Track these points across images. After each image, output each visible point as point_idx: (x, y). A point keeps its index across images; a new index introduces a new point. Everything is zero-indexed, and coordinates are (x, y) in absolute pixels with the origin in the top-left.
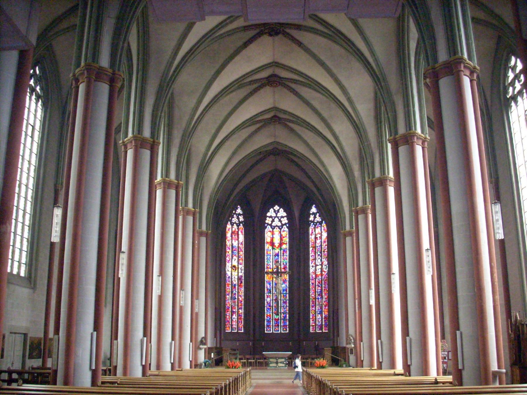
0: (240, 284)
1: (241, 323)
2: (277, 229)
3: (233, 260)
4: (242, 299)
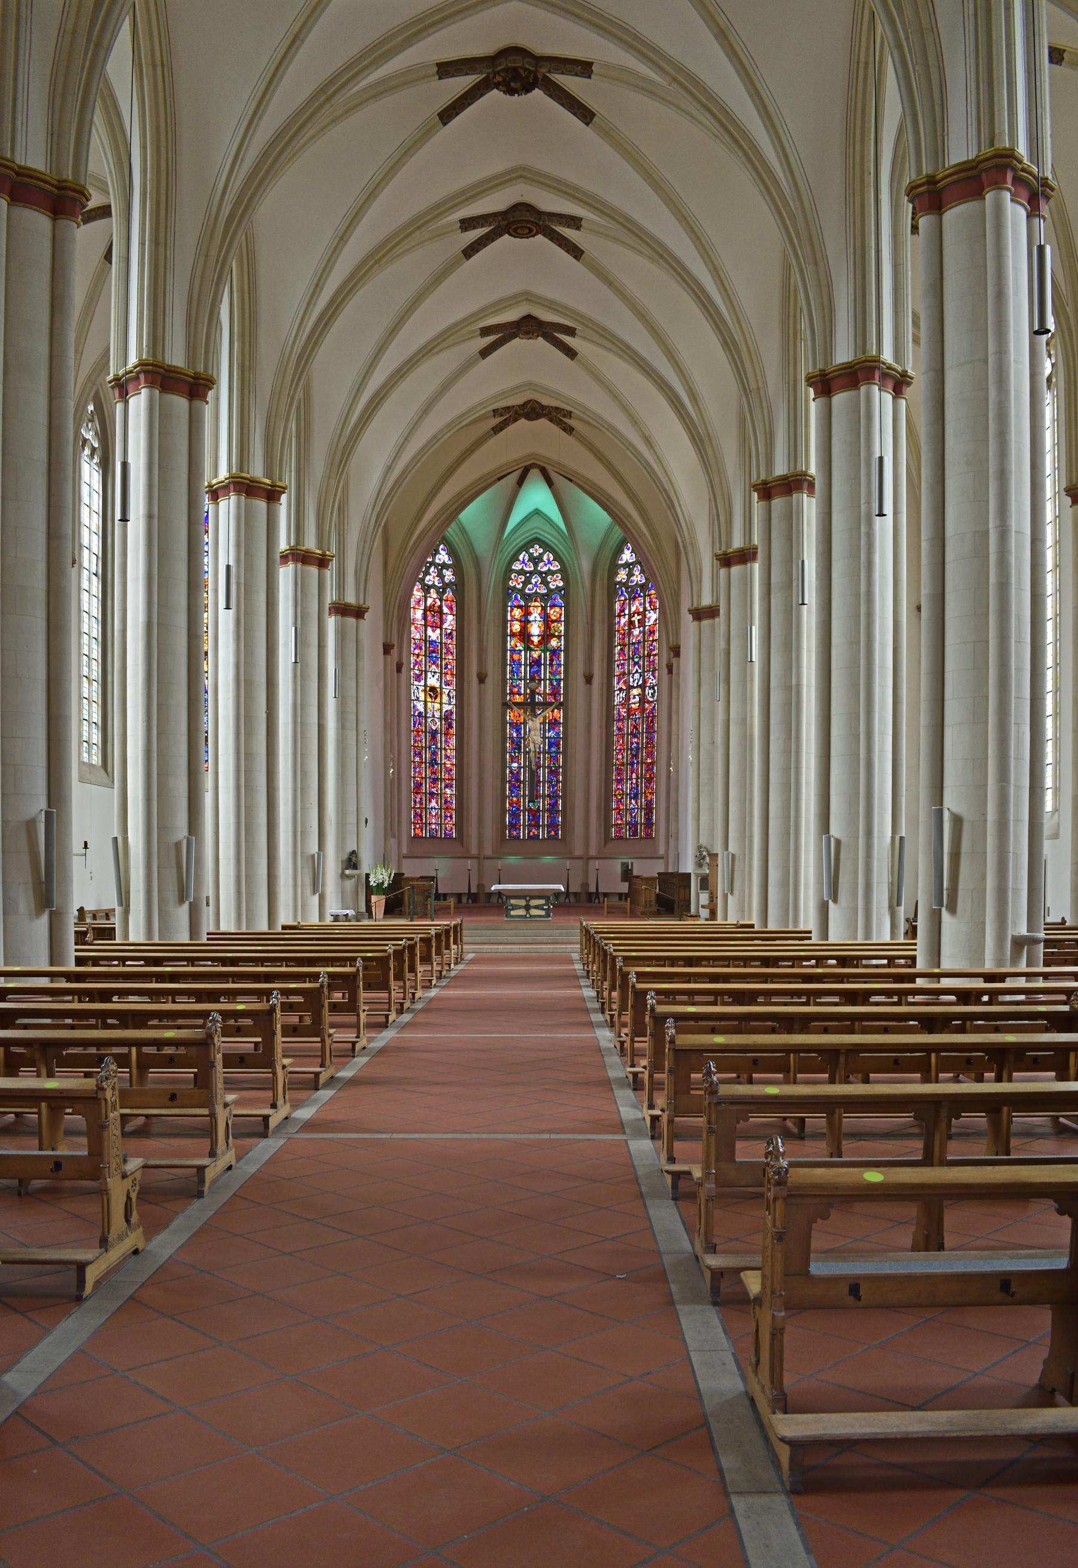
0: (447, 729)
1: (449, 819)
3: (429, 675)
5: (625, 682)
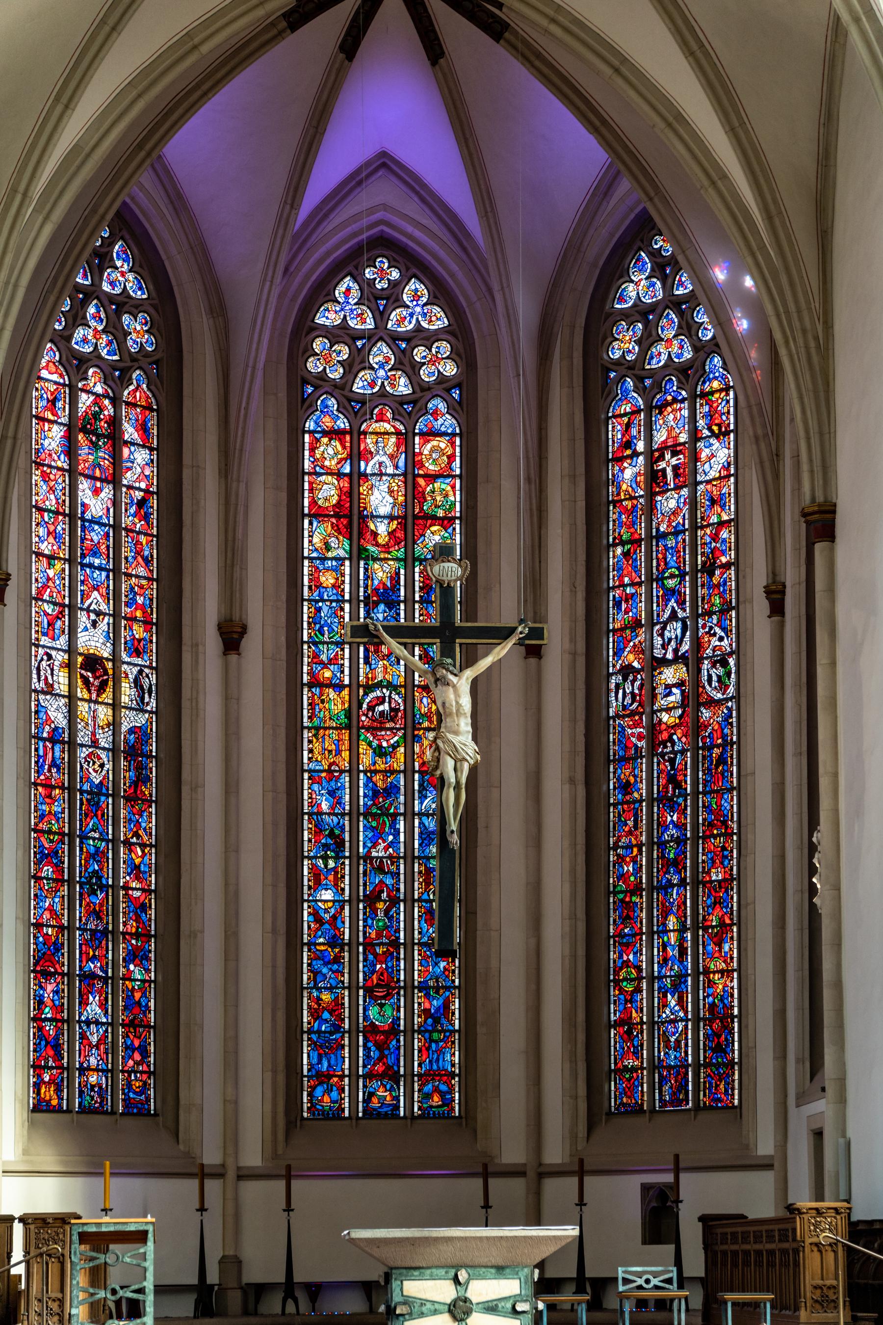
1: (137, 1056)
2: (381, 418)
3: (83, 619)
4: (146, 891)
5: (638, 650)
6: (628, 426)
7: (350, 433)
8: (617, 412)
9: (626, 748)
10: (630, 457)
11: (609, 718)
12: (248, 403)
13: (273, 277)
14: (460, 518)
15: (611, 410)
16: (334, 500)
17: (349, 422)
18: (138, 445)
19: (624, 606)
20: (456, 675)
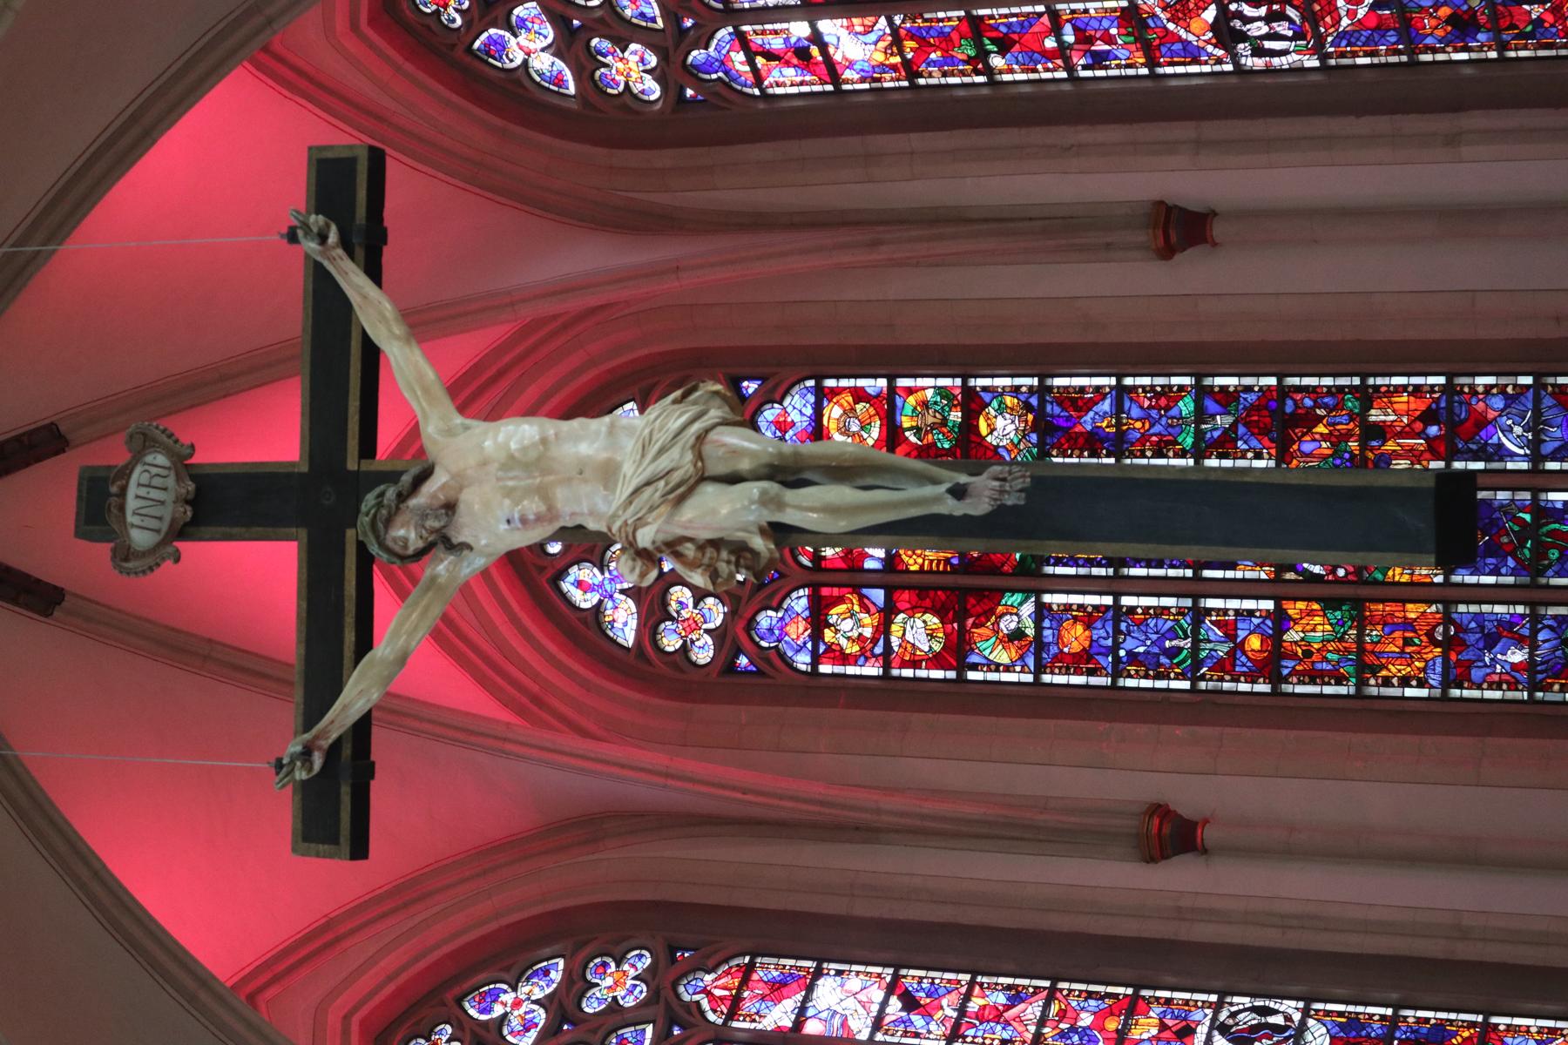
6: (770, 55)
7: (815, 588)
8: (750, 79)
9: (1381, 28)
10: (823, 47)
11: (1324, 68)
12: (734, 789)
13: (496, 738)
14: (965, 378)
15: (749, 90)
16: (933, 621)
17: (797, 589)
18: (806, 999)
19: (1100, 46)
20: (426, 474)
